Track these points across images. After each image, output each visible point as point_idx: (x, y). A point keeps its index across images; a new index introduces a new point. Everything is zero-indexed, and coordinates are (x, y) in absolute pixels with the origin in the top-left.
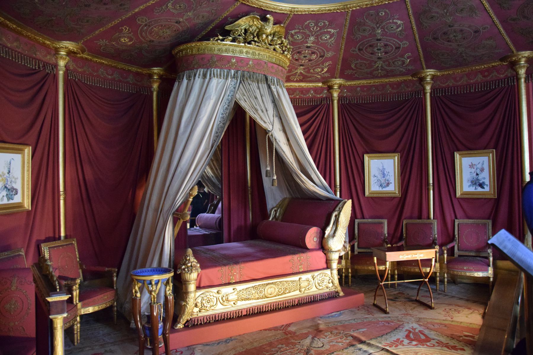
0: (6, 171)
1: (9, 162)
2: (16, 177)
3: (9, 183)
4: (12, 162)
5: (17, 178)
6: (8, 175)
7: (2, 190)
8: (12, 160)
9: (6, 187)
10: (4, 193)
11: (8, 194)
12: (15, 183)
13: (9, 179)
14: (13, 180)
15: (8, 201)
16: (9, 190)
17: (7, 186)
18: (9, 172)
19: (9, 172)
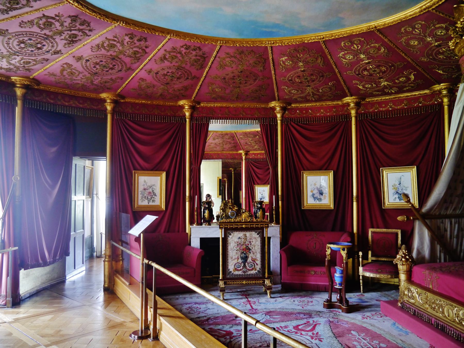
0: (397, 183)
1: (399, 177)
2: (406, 186)
3: (400, 190)
4: (402, 177)
5: (408, 187)
6: (399, 186)
7: (394, 194)
8: (402, 176)
9: (397, 193)
10: (397, 196)
11: (400, 196)
12: (406, 190)
13: (400, 188)
14: (404, 188)
15: (400, 201)
16: (400, 194)
17: (399, 192)
18: (400, 184)
19: (400, 184)
